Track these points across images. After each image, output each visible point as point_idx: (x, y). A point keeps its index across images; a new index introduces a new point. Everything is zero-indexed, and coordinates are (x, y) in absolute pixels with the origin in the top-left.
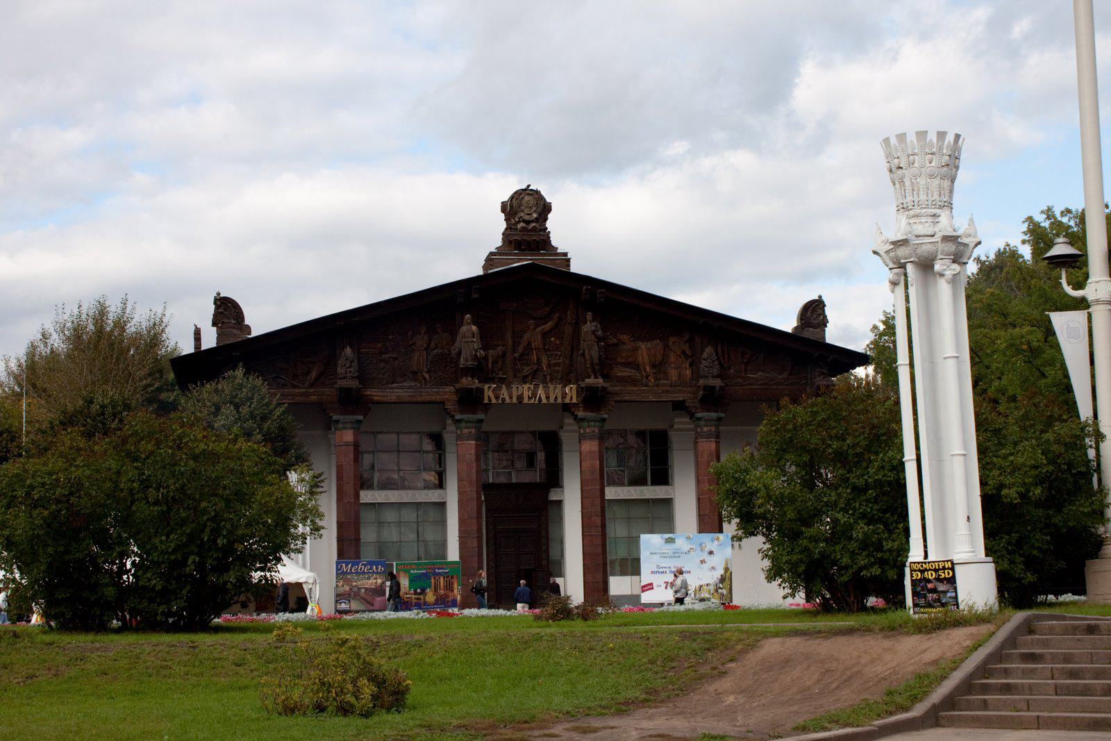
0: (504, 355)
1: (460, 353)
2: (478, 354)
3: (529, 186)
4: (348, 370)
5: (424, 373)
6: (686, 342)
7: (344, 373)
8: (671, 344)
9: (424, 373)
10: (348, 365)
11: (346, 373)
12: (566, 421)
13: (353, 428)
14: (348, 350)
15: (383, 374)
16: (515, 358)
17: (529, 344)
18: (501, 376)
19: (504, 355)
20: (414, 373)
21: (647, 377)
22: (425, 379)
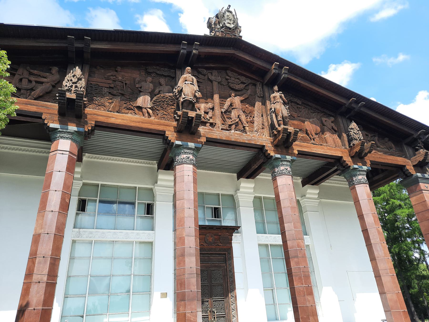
0: (213, 109)
1: (181, 91)
2: (197, 94)
3: (230, 6)
4: (74, 85)
5: (148, 109)
6: (332, 122)
7: (68, 85)
8: (324, 121)
9: (148, 109)
10: (75, 80)
11: (71, 86)
12: (242, 185)
13: (71, 139)
14: (78, 71)
15: (110, 103)
16: (222, 112)
17: (231, 105)
18: (211, 121)
19: (213, 109)
20: (140, 108)
21: (314, 139)
22: (148, 112)
